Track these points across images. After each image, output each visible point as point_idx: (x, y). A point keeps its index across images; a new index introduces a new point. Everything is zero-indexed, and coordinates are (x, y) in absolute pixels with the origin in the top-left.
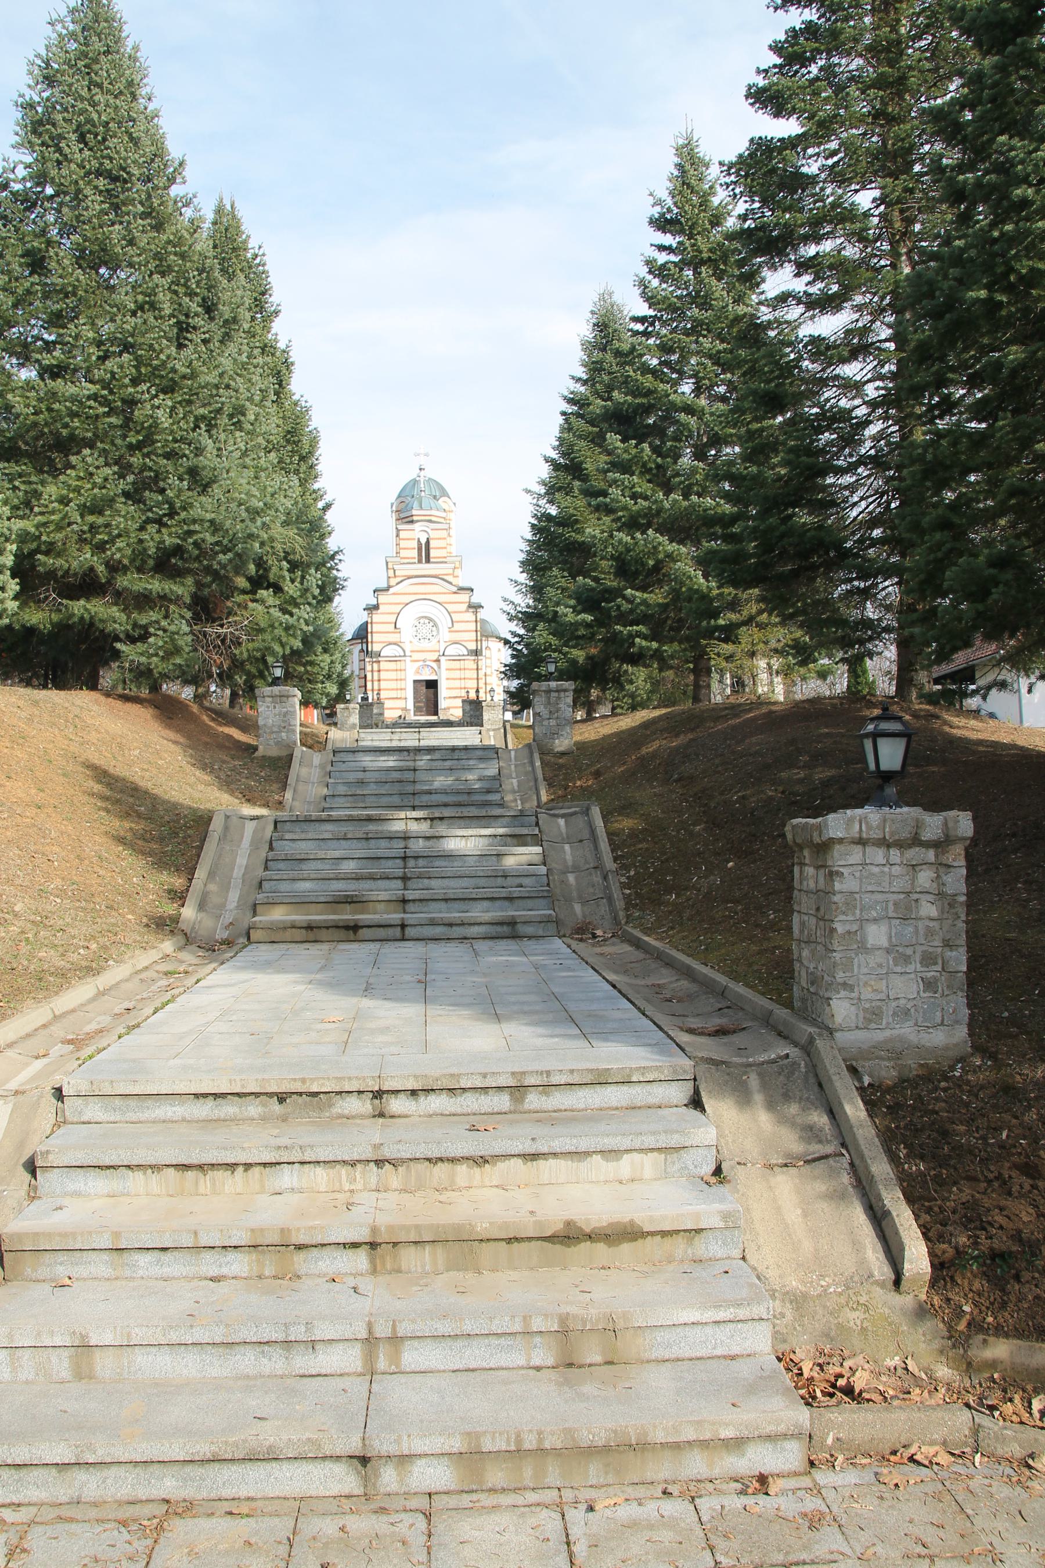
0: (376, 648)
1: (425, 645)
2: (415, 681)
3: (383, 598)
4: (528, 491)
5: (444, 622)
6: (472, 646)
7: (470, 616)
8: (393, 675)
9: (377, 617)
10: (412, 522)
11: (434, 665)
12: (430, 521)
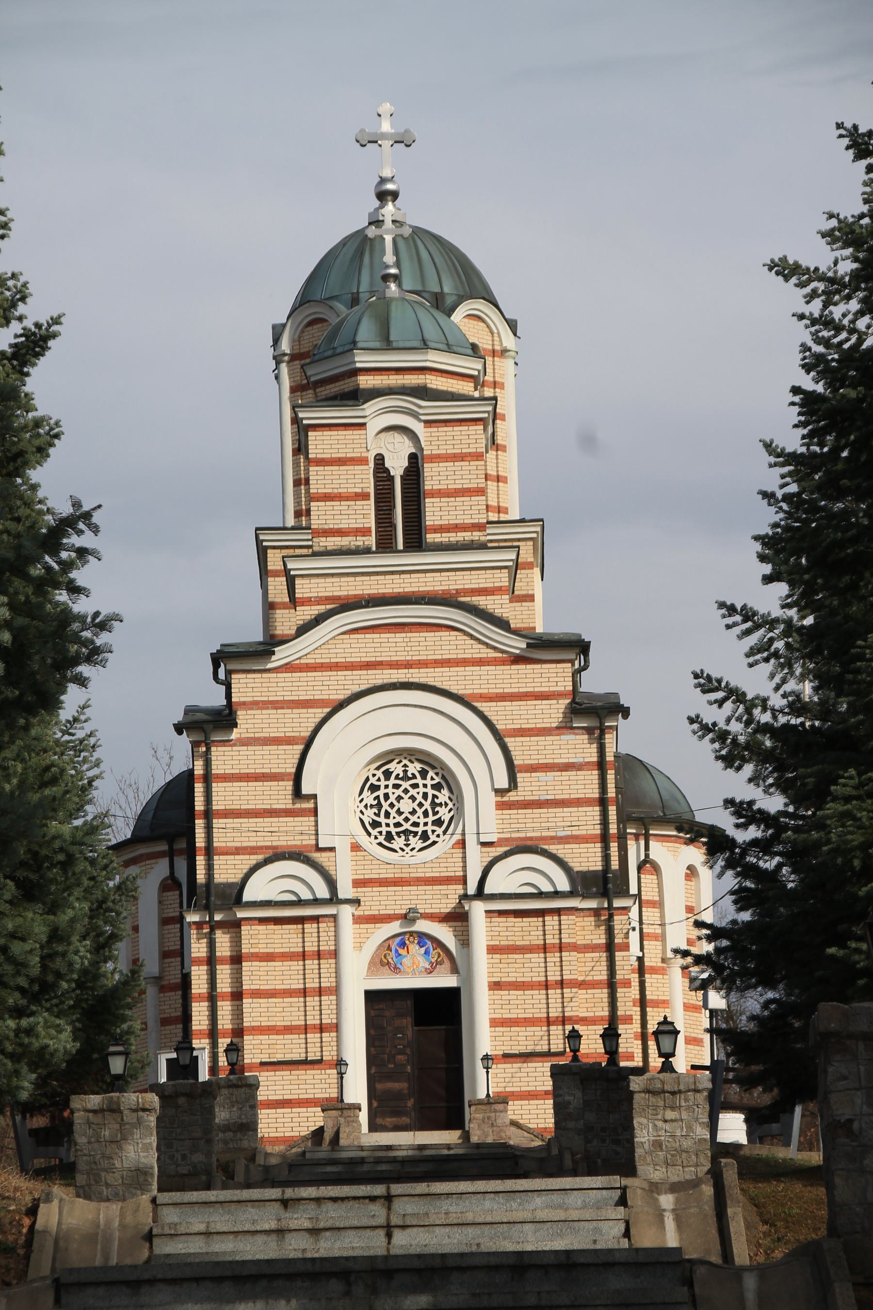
0: (227, 871)
2: (372, 997)
3: (246, 686)
4: (785, 269)
5: (478, 769)
6: (588, 859)
7: (578, 747)
8: (287, 975)
9: (223, 759)
10: (356, 397)
11: (445, 934)
12: (422, 393)
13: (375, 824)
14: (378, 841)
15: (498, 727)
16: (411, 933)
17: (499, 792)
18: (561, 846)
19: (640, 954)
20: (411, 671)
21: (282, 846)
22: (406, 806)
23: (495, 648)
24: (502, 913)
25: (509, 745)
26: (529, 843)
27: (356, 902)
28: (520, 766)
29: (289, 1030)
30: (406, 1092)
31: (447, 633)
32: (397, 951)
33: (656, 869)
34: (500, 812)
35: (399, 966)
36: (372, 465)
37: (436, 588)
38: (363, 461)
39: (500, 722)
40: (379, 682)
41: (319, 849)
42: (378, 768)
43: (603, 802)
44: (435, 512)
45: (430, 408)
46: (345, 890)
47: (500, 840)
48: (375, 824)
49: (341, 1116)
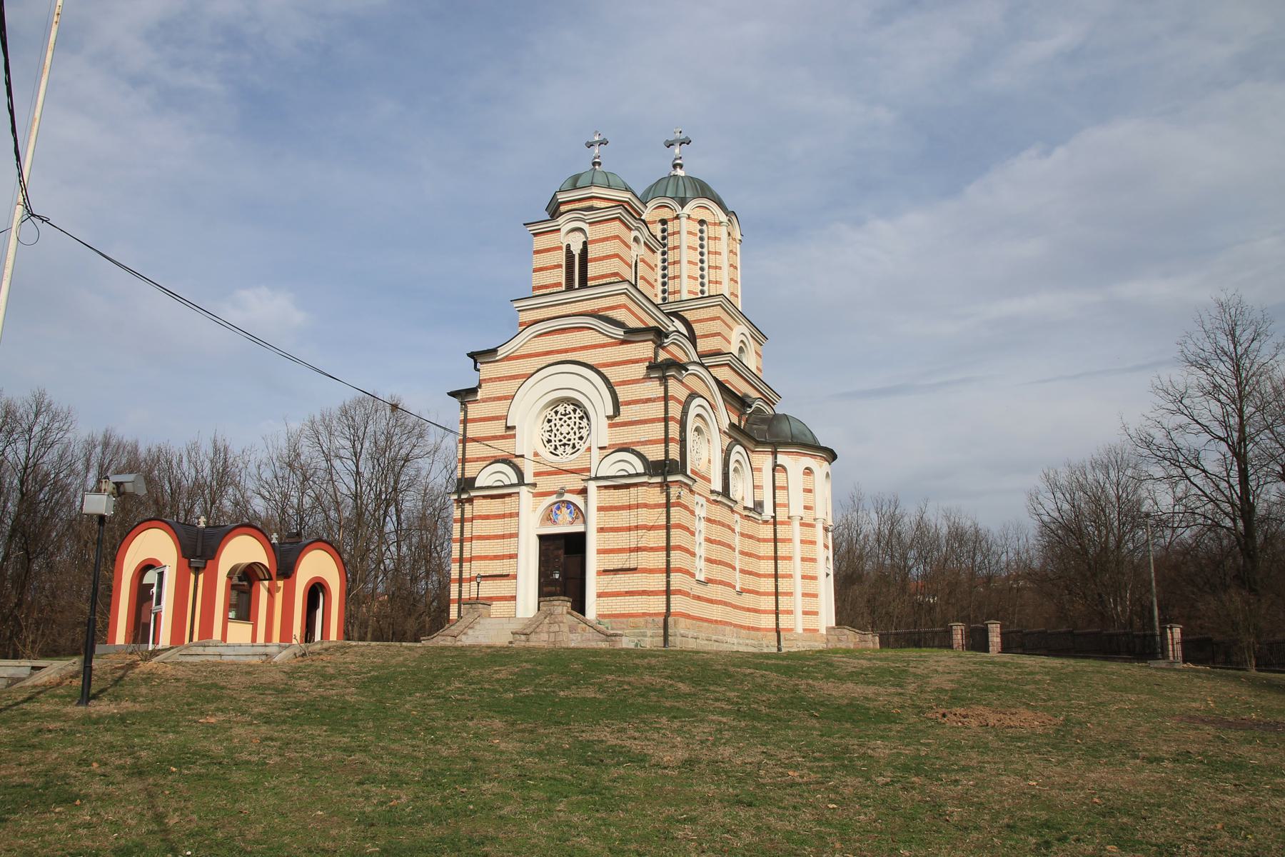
1: (567, 459)
2: (542, 538)
3: (487, 370)
5: (600, 405)
6: (656, 453)
9: (474, 410)
11: (578, 500)
12: (591, 209)
13: (549, 441)
16: (563, 502)
17: (608, 417)
22: (565, 429)
24: (606, 487)
27: (534, 485)
29: (496, 557)
38: (560, 248)
41: (517, 456)
43: (666, 420)
44: (592, 270)
45: (590, 215)
46: (529, 478)
48: (549, 441)
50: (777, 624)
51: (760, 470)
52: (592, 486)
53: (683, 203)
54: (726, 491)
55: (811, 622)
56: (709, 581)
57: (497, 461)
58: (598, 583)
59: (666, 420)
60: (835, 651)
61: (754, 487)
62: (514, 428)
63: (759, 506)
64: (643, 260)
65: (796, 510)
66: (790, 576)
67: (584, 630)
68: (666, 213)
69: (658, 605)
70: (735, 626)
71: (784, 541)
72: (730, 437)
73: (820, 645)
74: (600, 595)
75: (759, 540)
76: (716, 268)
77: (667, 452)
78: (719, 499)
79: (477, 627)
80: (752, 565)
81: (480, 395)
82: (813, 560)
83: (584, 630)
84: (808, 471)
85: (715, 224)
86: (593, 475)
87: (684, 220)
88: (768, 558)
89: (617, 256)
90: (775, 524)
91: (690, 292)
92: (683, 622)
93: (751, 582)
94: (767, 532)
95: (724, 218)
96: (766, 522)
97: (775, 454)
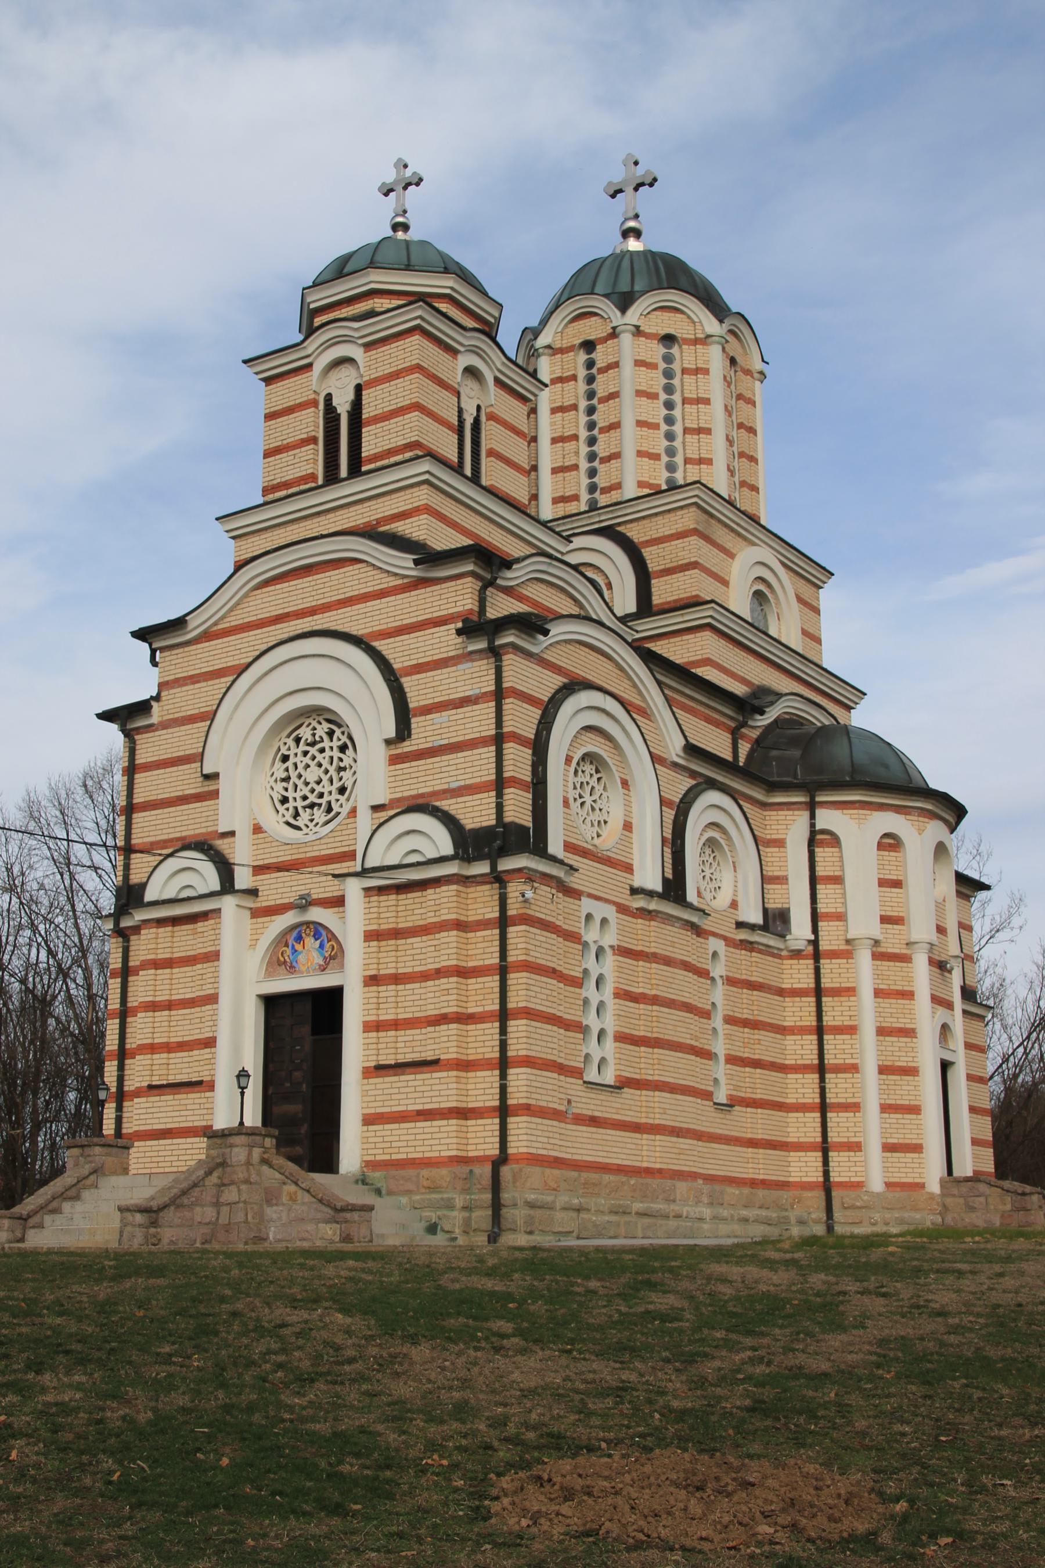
1: (316, 835)
2: (271, 1002)
6: (476, 813)
7: (477, 676)
9: (149, 749)
12: (371, 314)
14: (284, 819)
15: (395, 666)
16: (308, 924)
18: (453, 801)
19: (812, 937)
20: (316, 617)
21: (190, 836)
22: (312, 775)
23: (396, 574)
24: (381, 890)
25: (405, 685)
26: (420, 801)
27: (253, 892)
28: (415, 709)
30: (300, 1115)
31: (351, 568)
32: (293, 946)
33: (834, 840)
34: (393, 767)
35: (294, 964)
36: (321, 406)
37: (358, 522)
39: (398, 660)
40: (285, 636)
42: (289, 736)
44: (372, 441)
46: (243, 879)
47: (392, 801)
48: (284, 800)
49: (82, 1155)
50: (826, 1173)
51: (780, 843)
52: (353, 889)
53: (624, 302)
54: (674, 888)
55: (904, 1168)
56: (623, 1083)
57: (186, 847)
58: (365, 1093)
59: (499, 740)
60: (956, 1234)
61: (765, 879)
62: (213, 777)
63: (776, 921)
64: (492, 417)
65: (863, 923)
66: (854, 1068)
67: (293, 1198)
68: (591, 329)
69: (482, 1138)
70: (710, 1179)
71: (837, 992)
72: (693, 774)
73: (929, 1219)
74: (369, 1120)
75: (781, 992)
76: (699, 431)
77: (500, 808)
78: (653, 905)
79: (86, 1194)
80: (764, 1046)
81: (157, 714)
82: (909, 1033)
83: (293, 1198)
84: (890, 843)
85: (696, 341)
86: (359, 869)
87: (626, 339)
88: (802, 1031)
89: (417, 407)
90: (817, 956)
91: (641, 484)
92: (535, 1175)
93: (758, 1084)
94: (800, 974)
95: (711, 325)
96: (797, 954)
97: (812, 807)
